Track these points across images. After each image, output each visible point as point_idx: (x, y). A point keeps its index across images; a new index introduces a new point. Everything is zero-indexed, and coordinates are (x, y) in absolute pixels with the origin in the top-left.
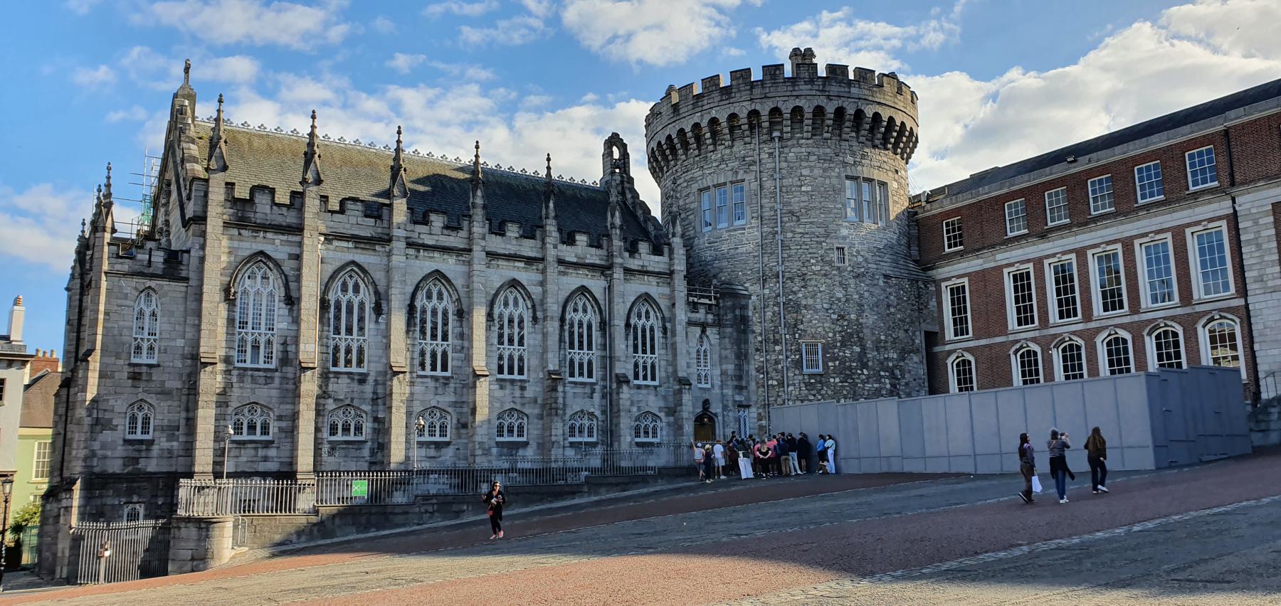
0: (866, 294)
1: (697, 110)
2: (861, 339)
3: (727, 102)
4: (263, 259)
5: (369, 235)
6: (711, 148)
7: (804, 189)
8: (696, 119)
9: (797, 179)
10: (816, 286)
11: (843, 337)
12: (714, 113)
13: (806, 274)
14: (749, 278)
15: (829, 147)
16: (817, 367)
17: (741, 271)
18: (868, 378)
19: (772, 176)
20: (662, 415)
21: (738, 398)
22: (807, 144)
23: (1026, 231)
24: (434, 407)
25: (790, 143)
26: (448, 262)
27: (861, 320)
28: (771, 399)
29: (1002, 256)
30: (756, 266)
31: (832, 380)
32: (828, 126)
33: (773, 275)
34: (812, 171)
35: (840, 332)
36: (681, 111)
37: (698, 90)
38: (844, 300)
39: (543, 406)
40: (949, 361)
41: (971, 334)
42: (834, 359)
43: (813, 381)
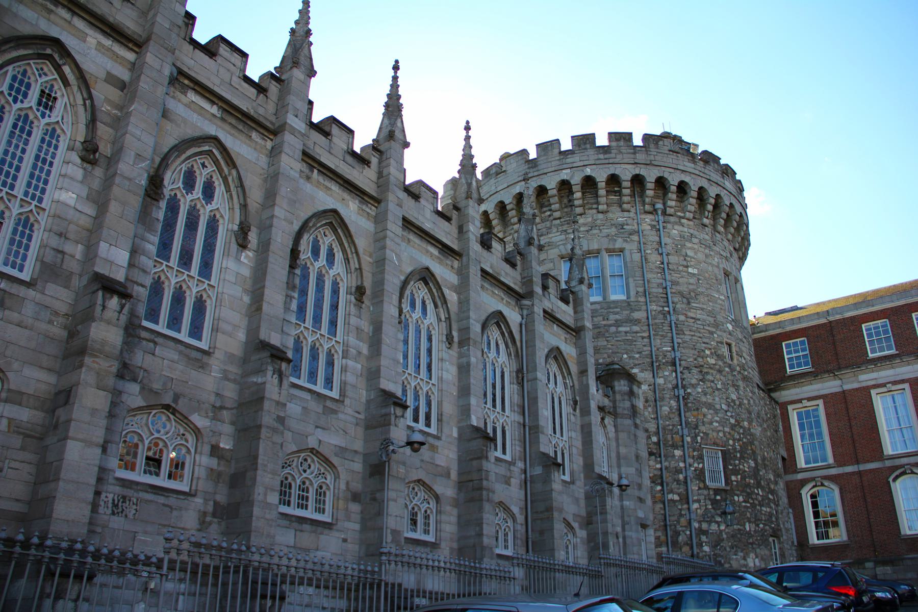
0: (752, 401)
1: (565, 166)
2: (754, 452)
4: (56, 56)
5: (245, 109)
6: (579, 210)
7: (690, 270)
8: (565, 175)
9: (682, 258)
10: (713, 382)
11: (741, 446)
12: (588, 171)
13: (702, 366)
14: (637, 362)
15: (707, 234)
16: (720, 481)
17: (627, 353)
18: (763, 500)
20: (575, 525)
21: (641, 514)
22: (688, 225)
23: (893, 351)
24: (312, 450)
25: (672, 219)
26: (348, 206)
27: (752, 430)
28: (673, 518)
29: (866, 378)
30: (645, 348)
31: (736, 498)
32: (709, 212)
33: (667, 362)
34: (696, 253)
35: (739, 440)
36: (540, 168)
38: (737, 403)
39: (461, 485)
41: (831, 460)
42: (736, 472)
43: (718, 497)
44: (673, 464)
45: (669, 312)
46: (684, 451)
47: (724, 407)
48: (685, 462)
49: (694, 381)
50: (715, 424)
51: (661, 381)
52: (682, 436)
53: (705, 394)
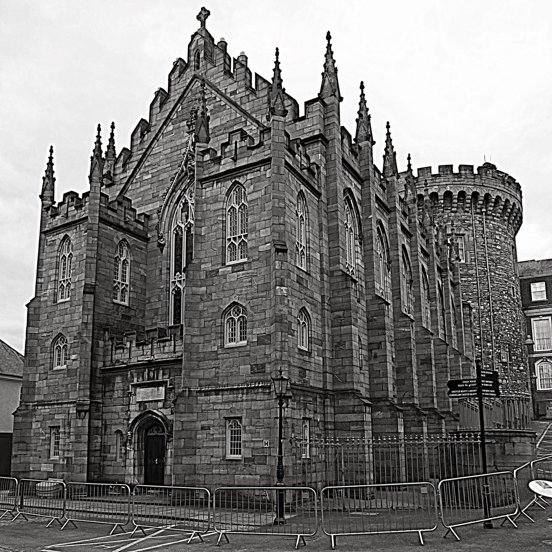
3: (459, 183)
10: (506, 308)
17: (465, 292)
19: (482, 235)
37: (435, 171)
40: (536, 364)
44: (487, 350)
45: (487, 271)
46: (492, 344)
47: (510, 321)
48: (492, 349)
49: (498, 308)
50: (506, 330)
51: (482, 307)
52: (492, 336)
53: (503, 315)
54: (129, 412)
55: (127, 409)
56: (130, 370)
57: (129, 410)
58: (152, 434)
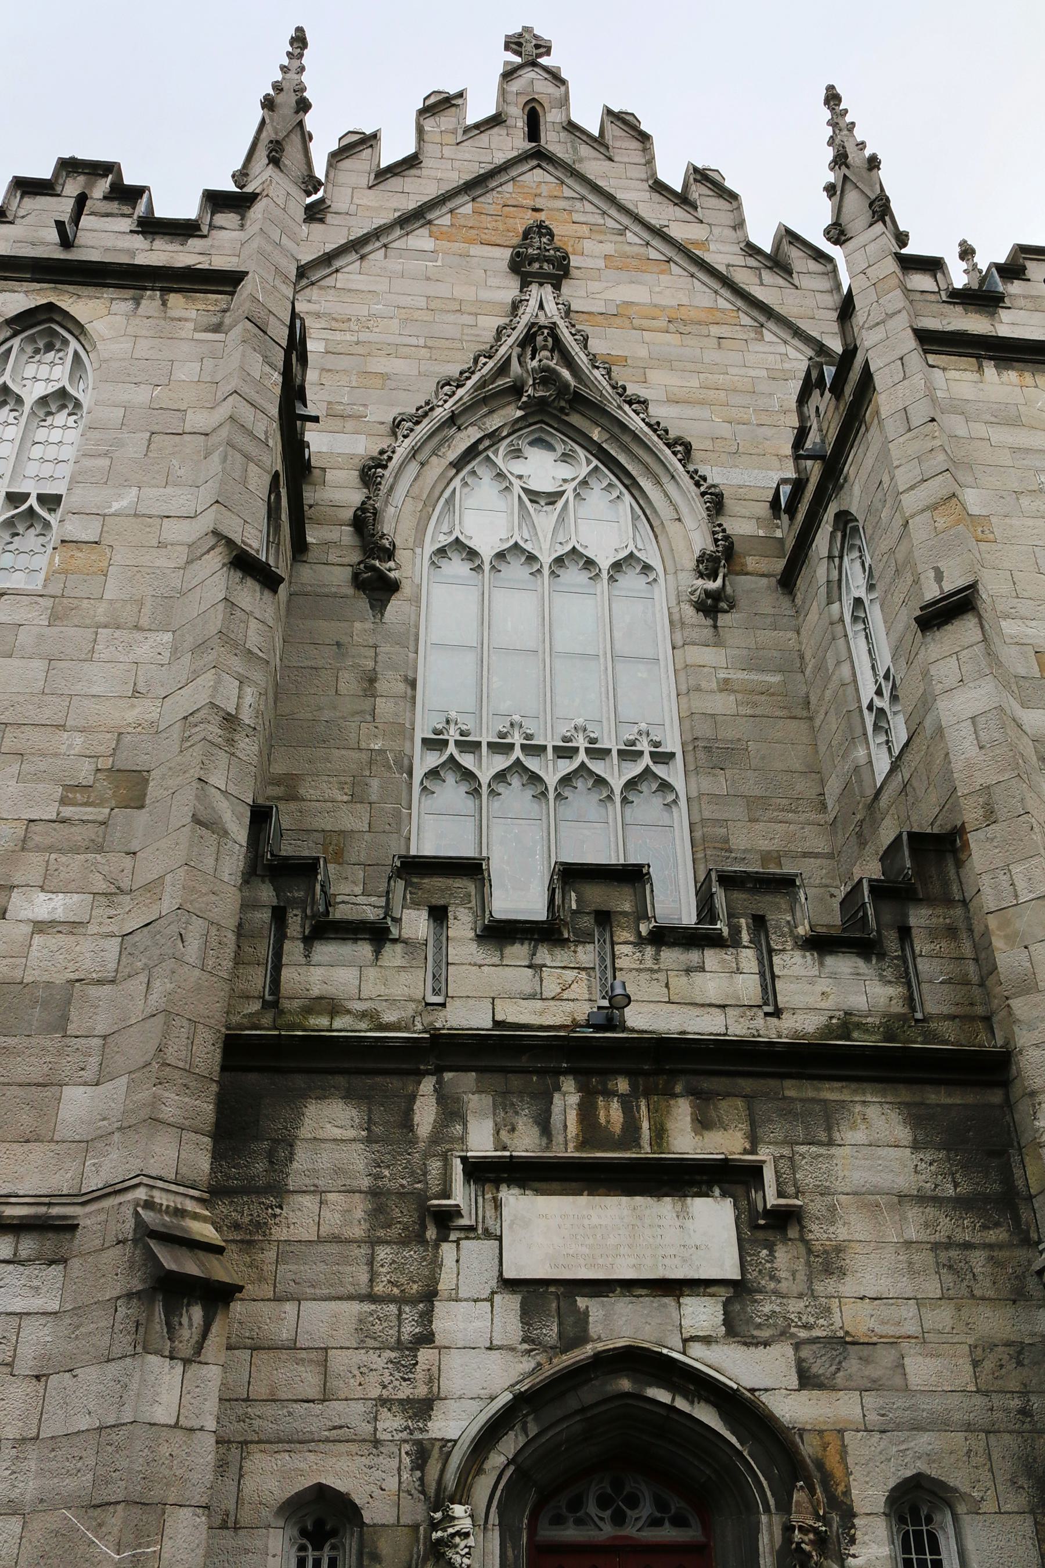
54: (425, 1355)
55: (410, 1329)
56: (438, 1071)
57: (426, 1338)
58: (571, 1533)
